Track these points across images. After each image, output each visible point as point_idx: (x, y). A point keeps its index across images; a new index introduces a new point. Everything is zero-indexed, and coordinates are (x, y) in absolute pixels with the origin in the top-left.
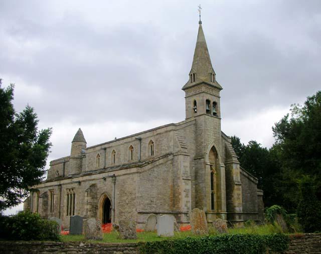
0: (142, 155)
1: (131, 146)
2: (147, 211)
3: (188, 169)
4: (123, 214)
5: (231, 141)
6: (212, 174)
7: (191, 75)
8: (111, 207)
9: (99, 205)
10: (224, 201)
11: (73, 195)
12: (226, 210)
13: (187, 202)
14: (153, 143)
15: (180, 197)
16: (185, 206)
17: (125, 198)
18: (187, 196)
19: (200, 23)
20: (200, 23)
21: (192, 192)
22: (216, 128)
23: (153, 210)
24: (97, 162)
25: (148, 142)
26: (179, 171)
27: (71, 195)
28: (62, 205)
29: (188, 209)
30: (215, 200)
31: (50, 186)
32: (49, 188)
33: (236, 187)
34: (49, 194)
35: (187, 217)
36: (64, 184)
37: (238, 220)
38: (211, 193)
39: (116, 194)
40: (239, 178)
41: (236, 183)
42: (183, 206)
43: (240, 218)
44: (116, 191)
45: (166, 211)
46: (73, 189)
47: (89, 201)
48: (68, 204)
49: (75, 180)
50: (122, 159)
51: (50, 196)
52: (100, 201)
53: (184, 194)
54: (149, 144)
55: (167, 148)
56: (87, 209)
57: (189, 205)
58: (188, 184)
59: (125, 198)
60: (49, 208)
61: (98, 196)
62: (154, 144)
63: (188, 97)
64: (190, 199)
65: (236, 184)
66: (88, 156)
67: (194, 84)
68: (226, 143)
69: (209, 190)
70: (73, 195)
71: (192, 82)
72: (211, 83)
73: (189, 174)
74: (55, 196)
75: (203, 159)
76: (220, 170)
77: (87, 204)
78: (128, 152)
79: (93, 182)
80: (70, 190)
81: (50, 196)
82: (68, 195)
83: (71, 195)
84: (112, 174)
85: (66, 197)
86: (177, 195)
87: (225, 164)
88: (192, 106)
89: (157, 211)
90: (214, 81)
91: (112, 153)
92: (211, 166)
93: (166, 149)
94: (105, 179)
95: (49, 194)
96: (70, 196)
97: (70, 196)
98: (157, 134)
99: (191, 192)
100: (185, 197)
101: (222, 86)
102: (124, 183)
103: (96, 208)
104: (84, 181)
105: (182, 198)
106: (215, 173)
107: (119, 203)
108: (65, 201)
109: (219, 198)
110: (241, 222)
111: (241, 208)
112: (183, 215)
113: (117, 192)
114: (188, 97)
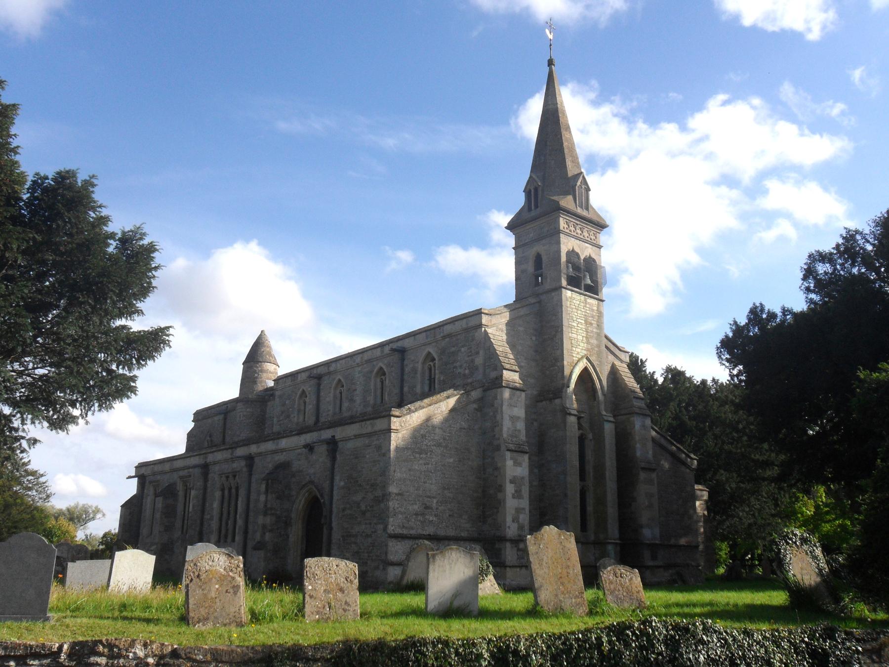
0: (406, 389)
1: (381, 368)
2: (413, 532)
3: (521, 426)
4: (353, 539)
5: (628, 360)
6: (582, 439)
7: (527, 192)
8: (323, 521)
9: (293, 515)
10: (612, 511)
11: (233, 491)
12: (617, 535)
13: (518, 510)
14: (433, 359)
15: (500, 496)
16: (513, 521)
17: (358, 497)
18: (518, 495)
19: (550, 63)
20: (550, 63)
21: (531, 486)
22: (591, 324)
23: (430, 530)
24: (299, 411)
25: (421, 359)
26: (497, 429)
27: (230, 489)
28: (207, 517)
29: (521, 528)
30: (590, 509)
31: (183, 469)
32: (181, 473)
33: (643, 475)
34: (180, 487)
35: (519, 550)
36: (215, 463)
37: (651, 563)
38: (579, 488)
39: (335, 488)
40: (651, 452)
41: (643, 465)
42: (509, 519)
43: (654, 557)
44: (337, 478)
45: (464, 534)
46: (235, 476)
47: (269, 506)
48: (222, 514)
49: (241, 452)
50: (358, 399)
51: (181, 494)
52: (300, 503)
53: (510, 489)
54: (424, 363)
55: (467, 372)
56: (264, 526)
57: (524, 518)
58: (520, 465)
59: (358, 497)
60: (178, 524)
61: (294, 493)
62: (436, 362)
63: (524, 245)
64: (525, 503)
65: (643, 469)
66: (280, 397)
67: (533, 213)
68: (617, 363)
69: (573, 479)
70: (233, 491)
71: (530, 209)
72: (579, 211)
73: (524, 438)
74: (193, 493)
75: (557, 401)
76: (602, 428)
77: (265, 514)
78: (372, 384)
79: (280, 458)
80: (227, 477)
81: (181, 494)
82: (223, 490)
83: (230, 489)
84: (327, 434)
85: (218, 494)
86: (492, 492)
87: (614, 416)
88: (530, 267)
89: (441, 533)
90: (587, 206)
91: (336, 388)
92: (579, 418)
93: (464, 375)
94: (310, 447)
95: (180, 487)
96: (226, 492)
97: (226, 492)
98: (444, 337)
99: (527, 484)
100: (514, 497)
101: (607, 219)
102: (356, 458)
103: (287, 523)
104: (260, 454)
105: (504, 500)
106: (590, 436)
107: (344, 510)
108: (216, 505)
109: (601, 501)
110: (658, 567)
111: (657, 531)
112: (508, 545)
113: (339, 482)
114: (524, 245)
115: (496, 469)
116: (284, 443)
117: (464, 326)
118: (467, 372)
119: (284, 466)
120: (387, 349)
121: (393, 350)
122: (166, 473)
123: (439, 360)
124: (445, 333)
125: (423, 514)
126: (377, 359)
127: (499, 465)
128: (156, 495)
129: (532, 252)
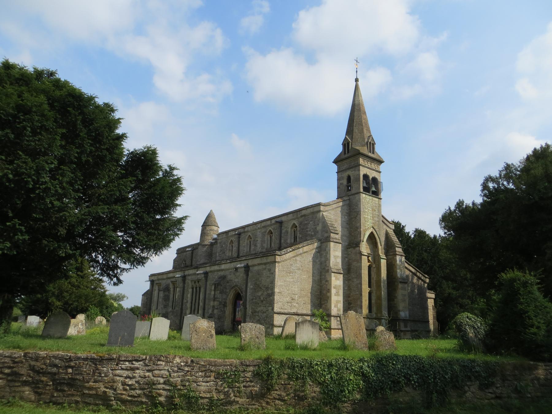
0: (282, 241)
6: (370, 267)
10: (385, 303)
11: (198, 289)
14: (296, 227)
15: (328, 294)
18: (337, 294)
21: (344, 289)
22: (375, 210)
24: (229, 250)
25: (290, 227)
27: (196, 288)
28: (185, 301)
30: (373, 301)
33: (400, 286)
34: (171, 286)
36: (189, 275)
37: (403, 329)
39: (248, 289)
41: (400, 280)
43: (406, 326)
44: (249, 284)
46: (198, 282)
48: (192, 300)
50: (259, 245)
51: (172, 290)
53: (333, 291)
54: (292, 228)
55: (313, 233)
56: (213, 307)
58: (338, 279)
59: (260, 294)
61: (228, 291)
64: (341, 298)
65: (401, 282)
66: (220, 243)
67: (347, 156)
68: (388, 229)
70: (198, 289)
71: (345, 153)
72: (370, 155)
73: (341, 267)
74: (178, 289)
80: (195, 282)
81: (172, 290)
82: (193, 288)
83: (196, 288)
85: (190, 290)
88: (345, 182)
92: (368, 257)
93: (312, 235)
95: (171, 286)
96: (194, 289)
97: (194, 289)
98: (302, 216)
99: (342, 289)
100: (335, 295)
103: (225, 305)
104: (211, 271)
106: (374, 266)
108: (189, 296)
111: (407, 313)
113: (250, 286)
115: (327, 281)
116: (223, 267)
117: (312, 211)
118: (313, 233)
119: (224, 277)
120: (273, 221)
121: (277, 222)
122: (164, 279)
123: (300, 227)
124: (303, 214)
125: (291, 303)
126: (268, 226)
127: (328, 279)
128: (159, 290)
129: (345, 175)
